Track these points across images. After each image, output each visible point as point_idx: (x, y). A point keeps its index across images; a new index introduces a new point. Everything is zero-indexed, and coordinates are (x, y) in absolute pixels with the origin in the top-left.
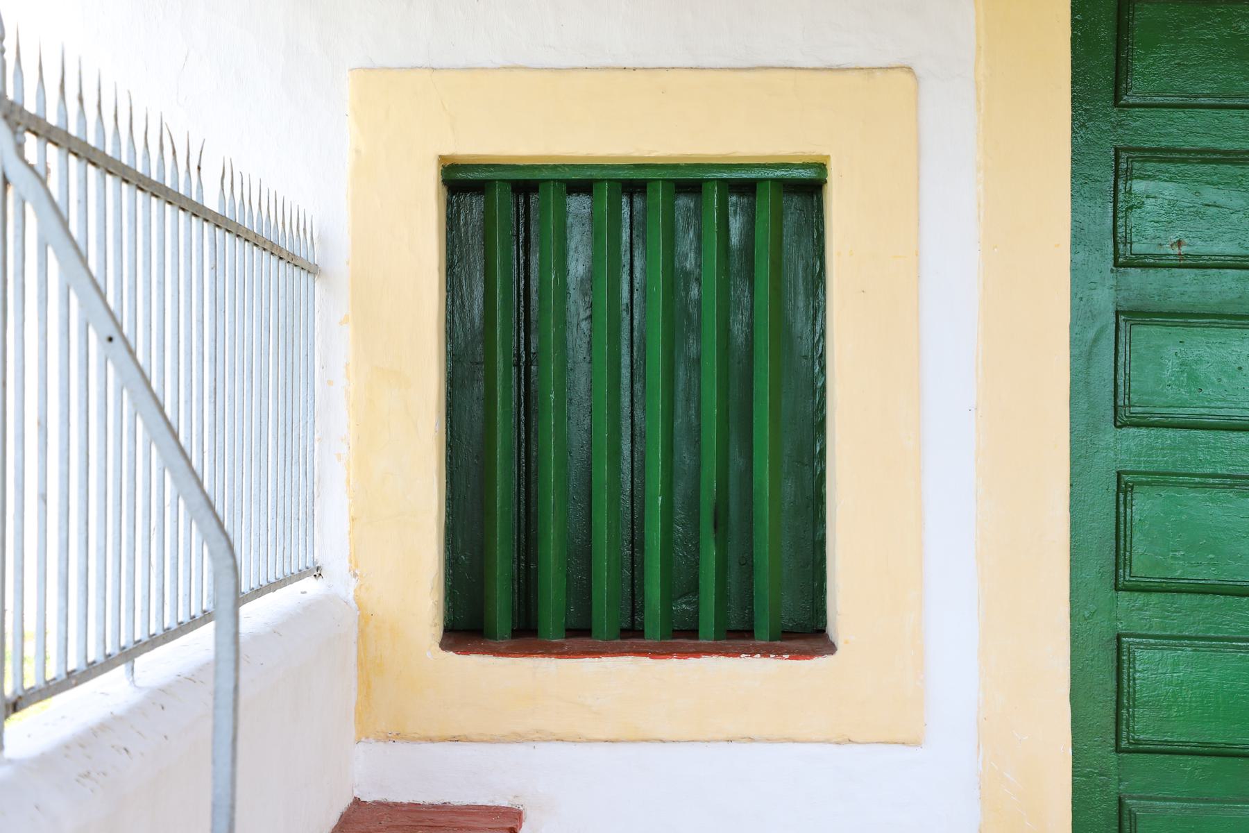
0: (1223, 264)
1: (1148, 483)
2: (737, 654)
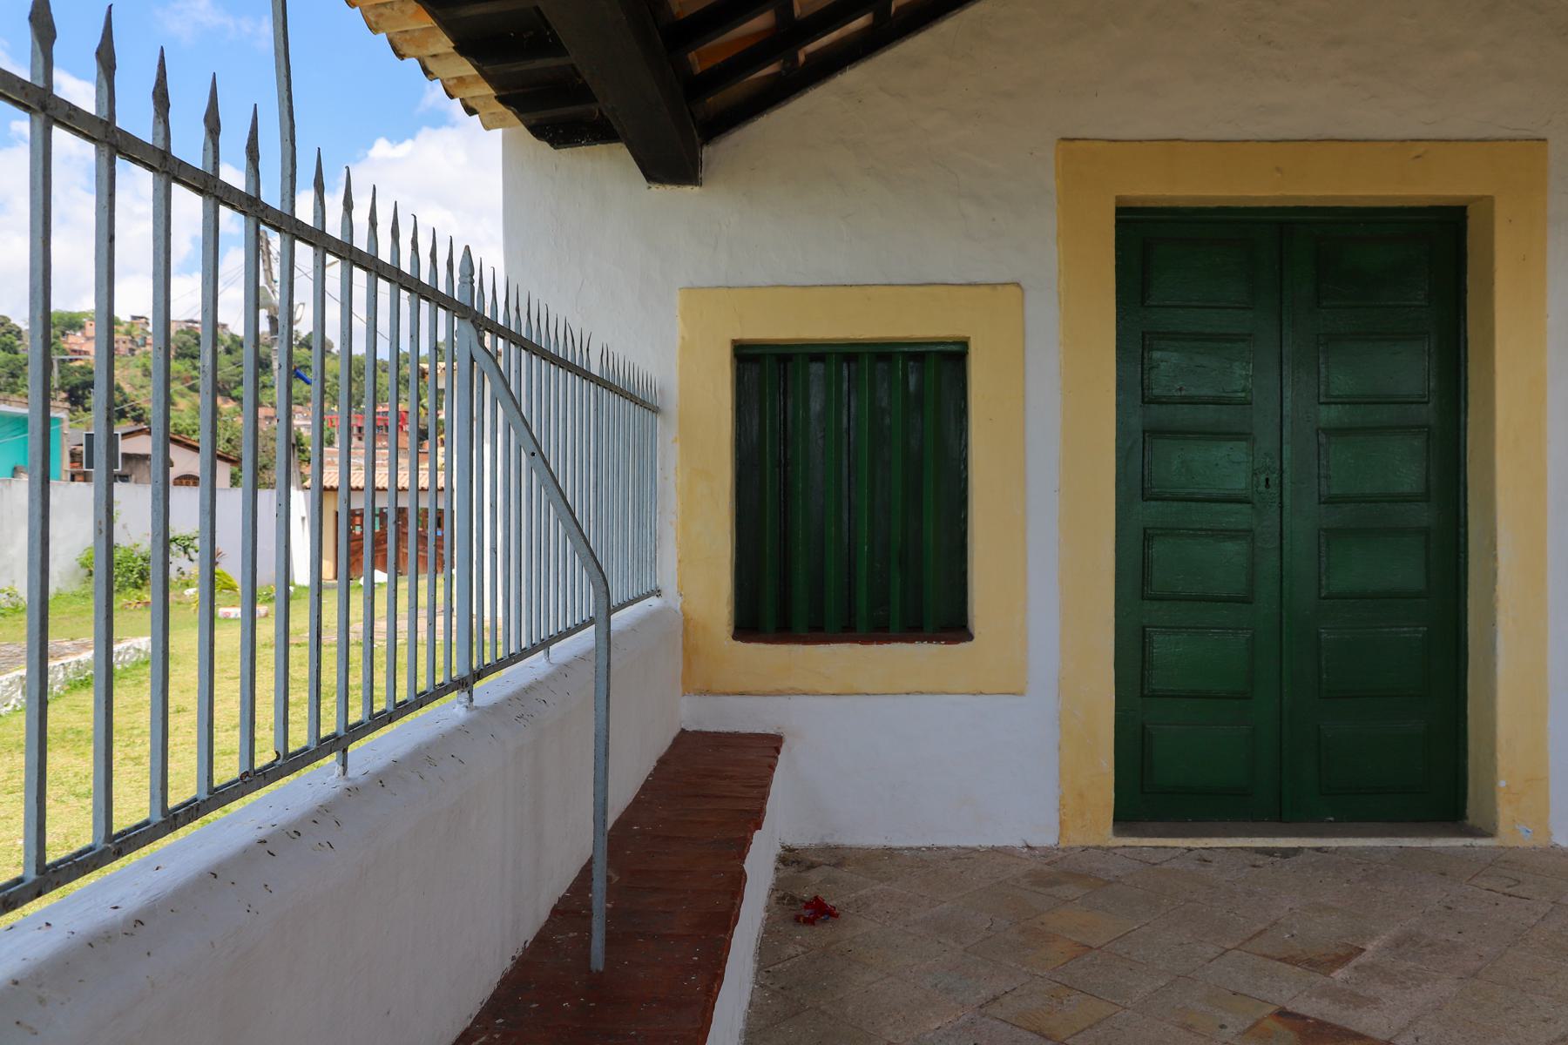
2: (912, 641)
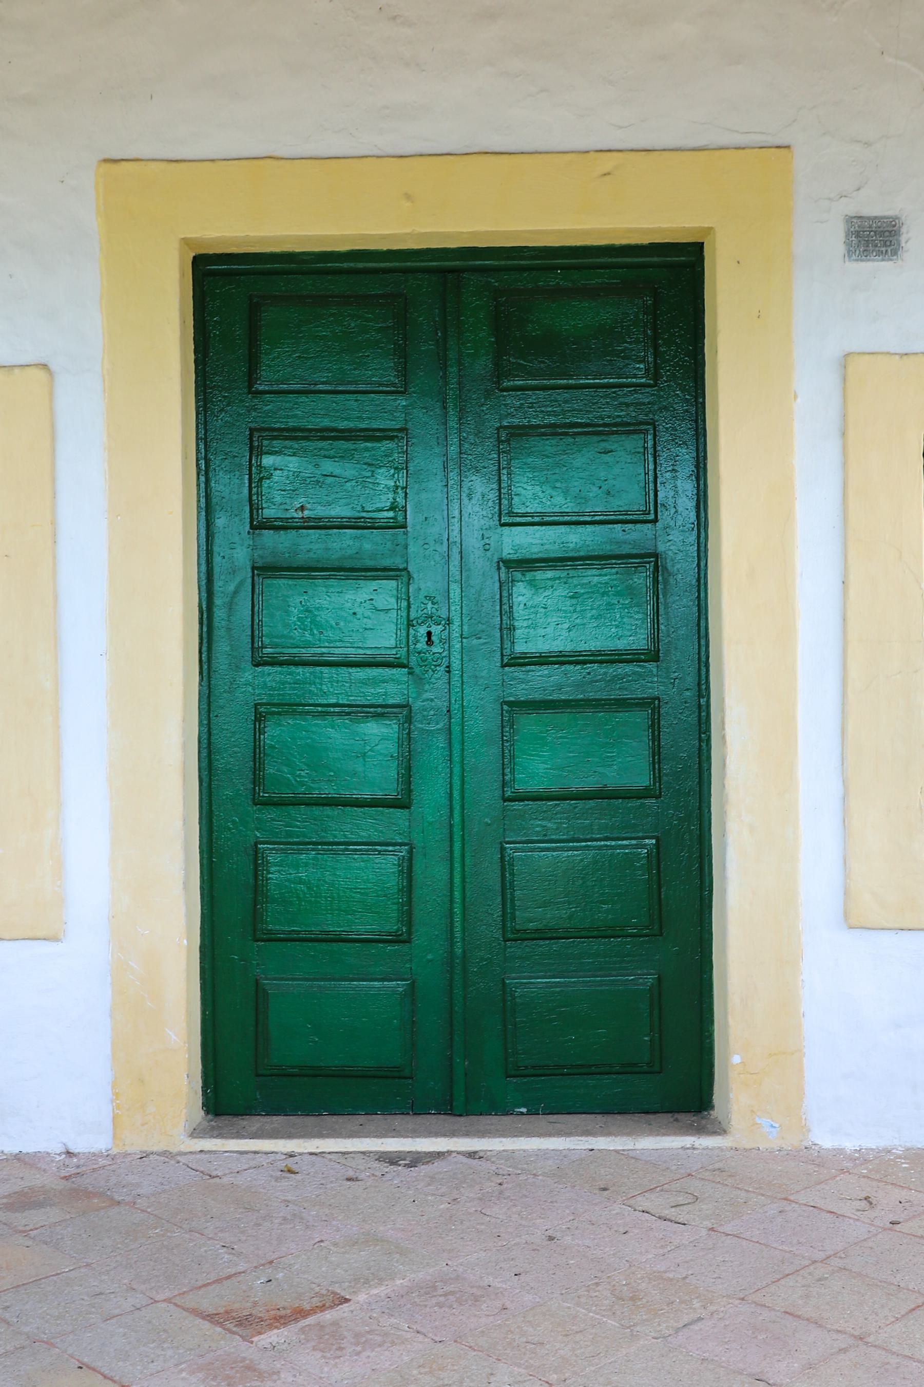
1: (279, 713)
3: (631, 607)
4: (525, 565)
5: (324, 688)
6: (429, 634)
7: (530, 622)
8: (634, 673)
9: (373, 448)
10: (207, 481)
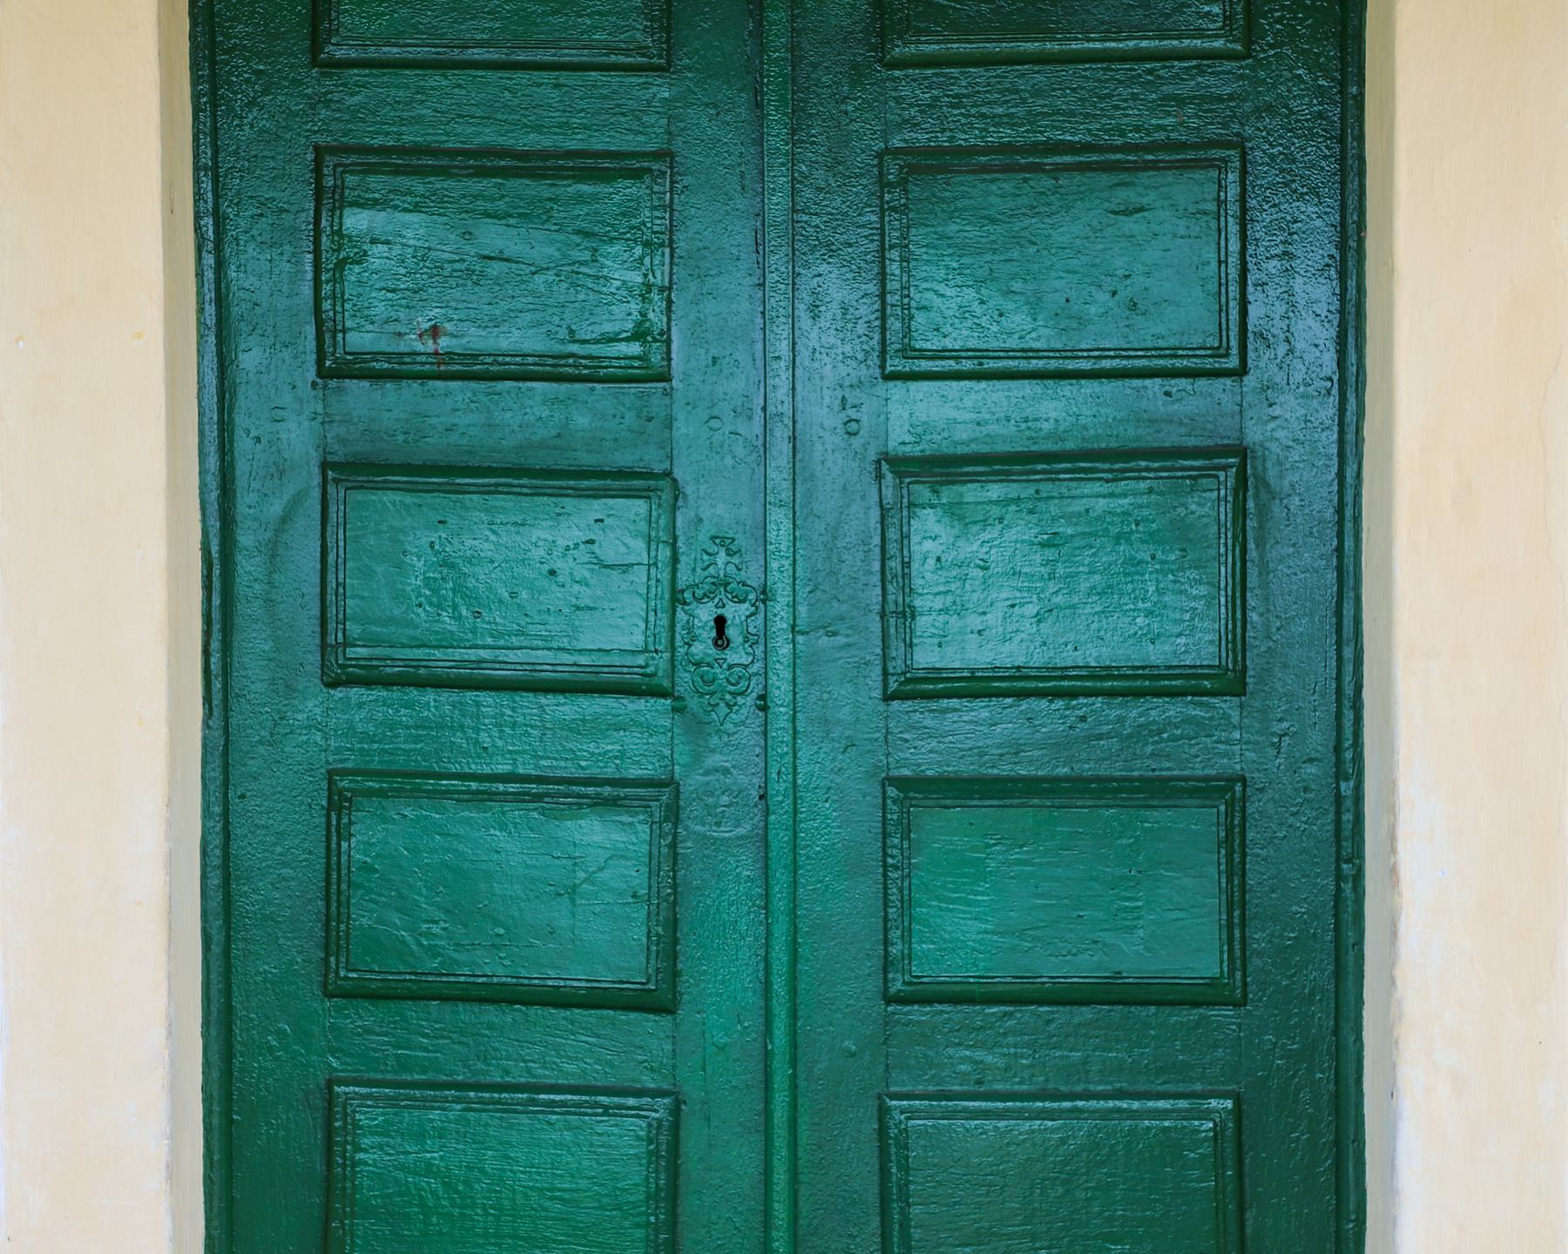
0: (523, 372)
3: (1183, 569)
4: (939, 468)
5: (484, 738)
6: (720, 622)
7: (950, 598)
8: (1188, 720)
9: (595, 198)
10: (220, 266)
